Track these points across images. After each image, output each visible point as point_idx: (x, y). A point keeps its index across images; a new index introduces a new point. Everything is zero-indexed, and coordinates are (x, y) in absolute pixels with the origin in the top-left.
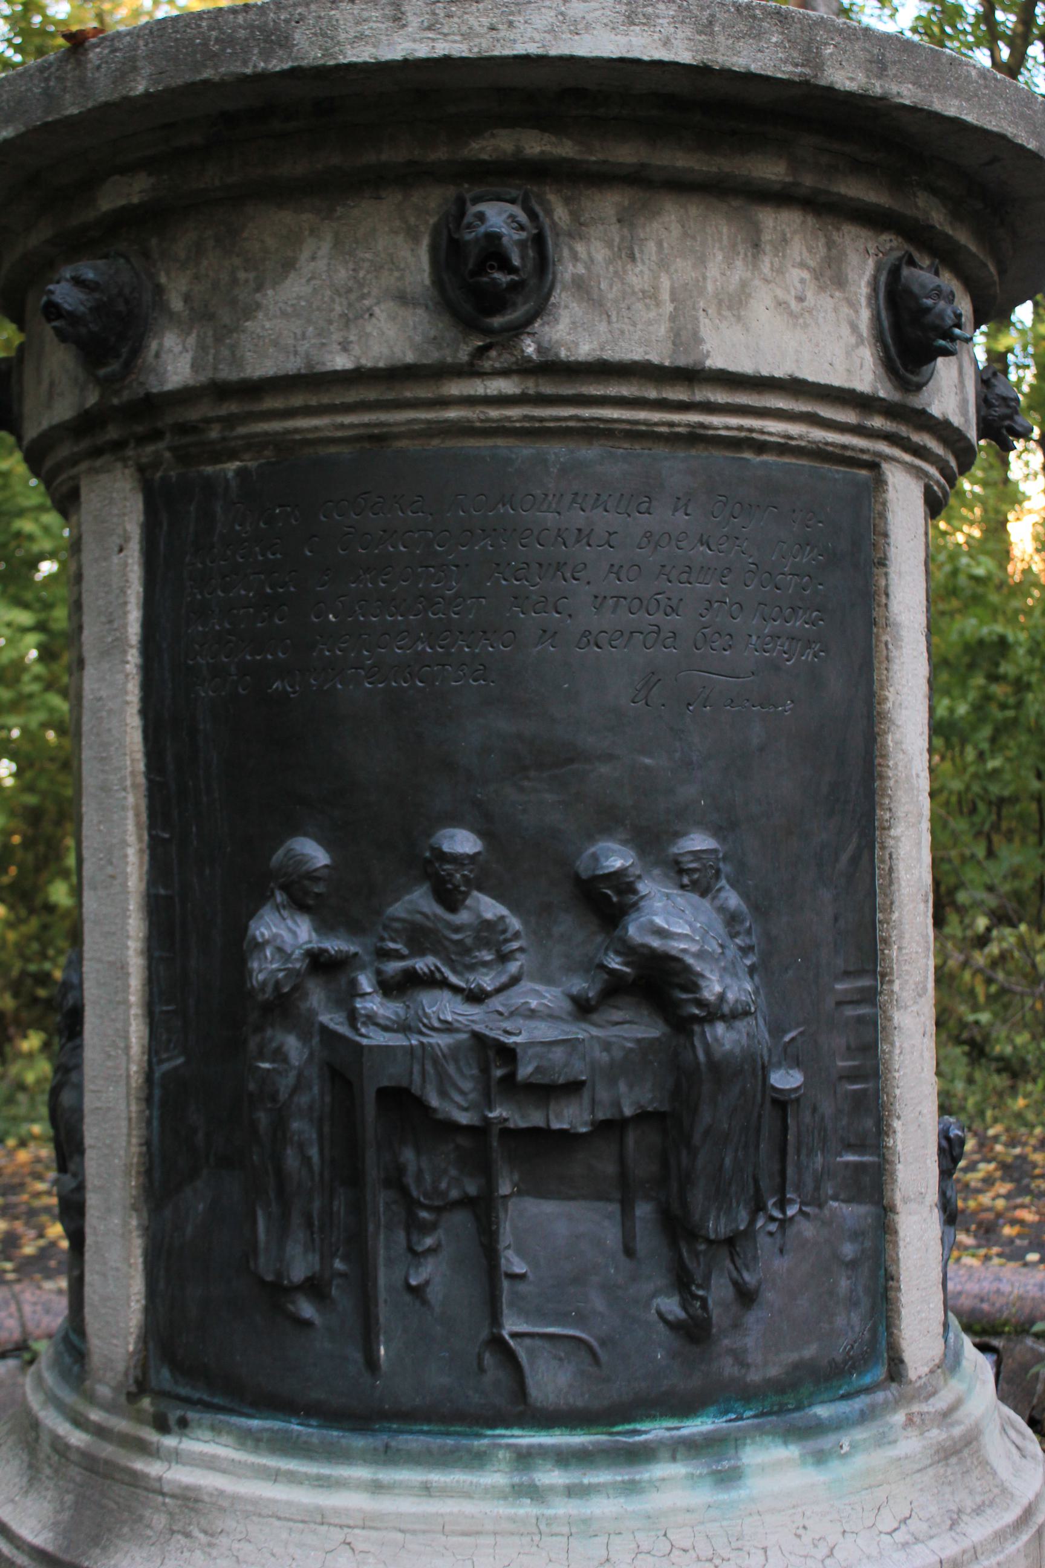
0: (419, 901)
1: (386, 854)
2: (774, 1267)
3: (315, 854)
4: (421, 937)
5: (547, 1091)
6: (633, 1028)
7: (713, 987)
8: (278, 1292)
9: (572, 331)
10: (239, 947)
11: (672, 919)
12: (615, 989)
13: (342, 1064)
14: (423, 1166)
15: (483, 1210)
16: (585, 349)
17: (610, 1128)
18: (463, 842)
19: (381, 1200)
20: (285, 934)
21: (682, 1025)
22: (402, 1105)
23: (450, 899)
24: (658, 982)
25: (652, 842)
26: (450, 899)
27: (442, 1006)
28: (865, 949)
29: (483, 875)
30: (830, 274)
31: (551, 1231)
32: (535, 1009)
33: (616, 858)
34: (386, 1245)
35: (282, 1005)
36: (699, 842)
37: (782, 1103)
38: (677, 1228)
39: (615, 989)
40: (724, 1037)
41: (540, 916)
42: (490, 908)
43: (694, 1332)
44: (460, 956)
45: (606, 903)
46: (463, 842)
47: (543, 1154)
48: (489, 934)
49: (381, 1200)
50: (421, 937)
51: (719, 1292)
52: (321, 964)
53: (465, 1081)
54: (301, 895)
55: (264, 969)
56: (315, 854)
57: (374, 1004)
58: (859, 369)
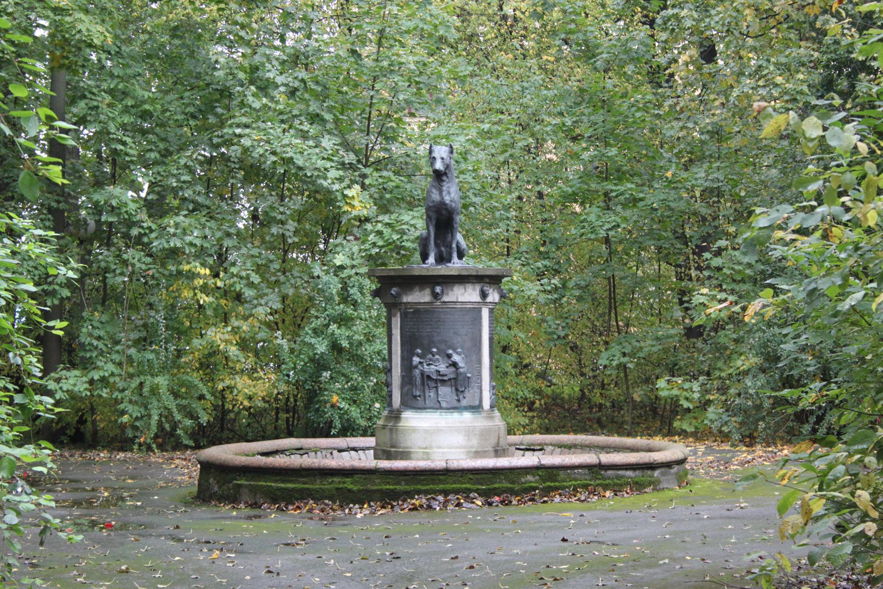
0: (430, 356)
1: (427, 351)
2: (467, 394)
3: (419, 351)
4: (430, 360)
5: (443, 375)
6: (452, 369)
7: (460, 365)
8: (415, 397)
9: (446, 299)
10: (411, 361)
11: (456, 358)
12: (450, 365)
13: (422, 373)
14: (432, 384)
15: (436, 387)
16: (446, 300)
17: (450, 379)
18: (435, 350)
19: (426, 387)
20: (416, 360)
21: (457, 369)
22: (429, 377)
23: (433, 356)
24: (454, 365)
25: (455, 350)
26: (433, 356)
27: (433, 367)
28: (480, 361)
29: (437, 353)
30: (474, 290)
31: (445, 391)
32: (442, 367)
33: (450, 352)
34: (427, 391)
35: (416, 367)
36: (459, 350)
37: (469, 378)
38: (457, 390)
39: (450, 365)
40: (461, 370)
41: (443, 358)
42: (437, 357)
43: (459, 401)
44: (435, 362)
45: (449, 356)
46: (435, 350)
47: (443, 381)
48: (437, 359)
49: (426, 387)
50: (430, 360)
51: (461, 397)
52: (421, 363)
53: (435, 374)
54: (418, 355)
55: (414, 363)
56: (419, 351)
57: (425, 366)
58: (478, 299)
